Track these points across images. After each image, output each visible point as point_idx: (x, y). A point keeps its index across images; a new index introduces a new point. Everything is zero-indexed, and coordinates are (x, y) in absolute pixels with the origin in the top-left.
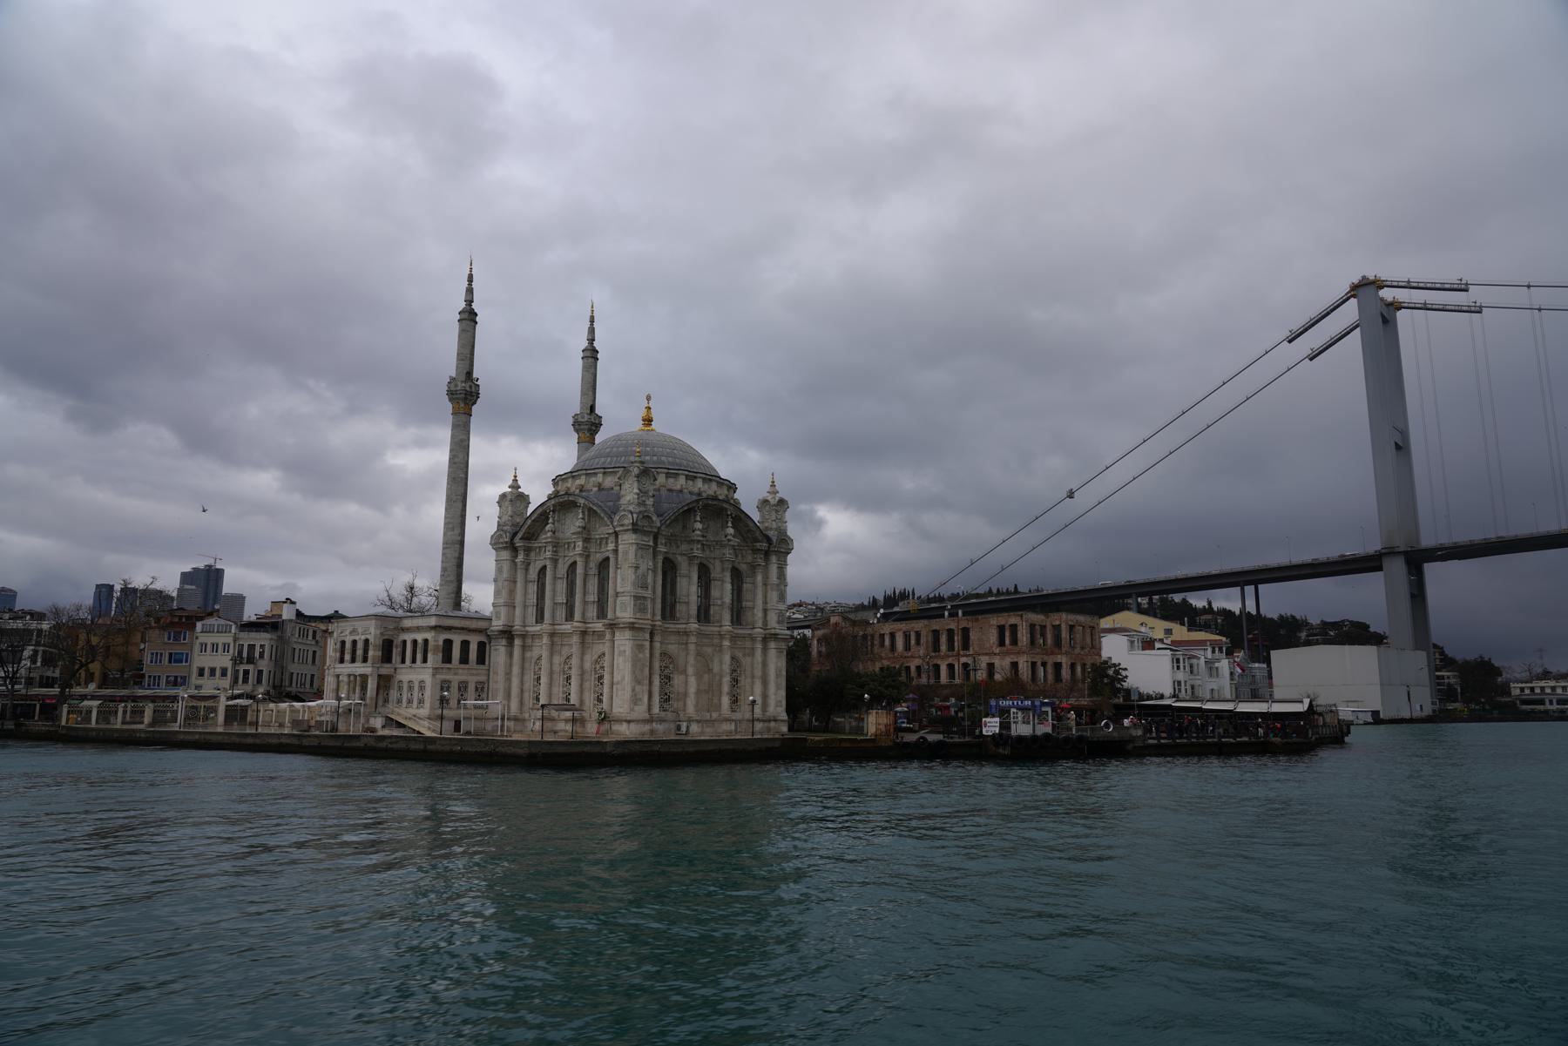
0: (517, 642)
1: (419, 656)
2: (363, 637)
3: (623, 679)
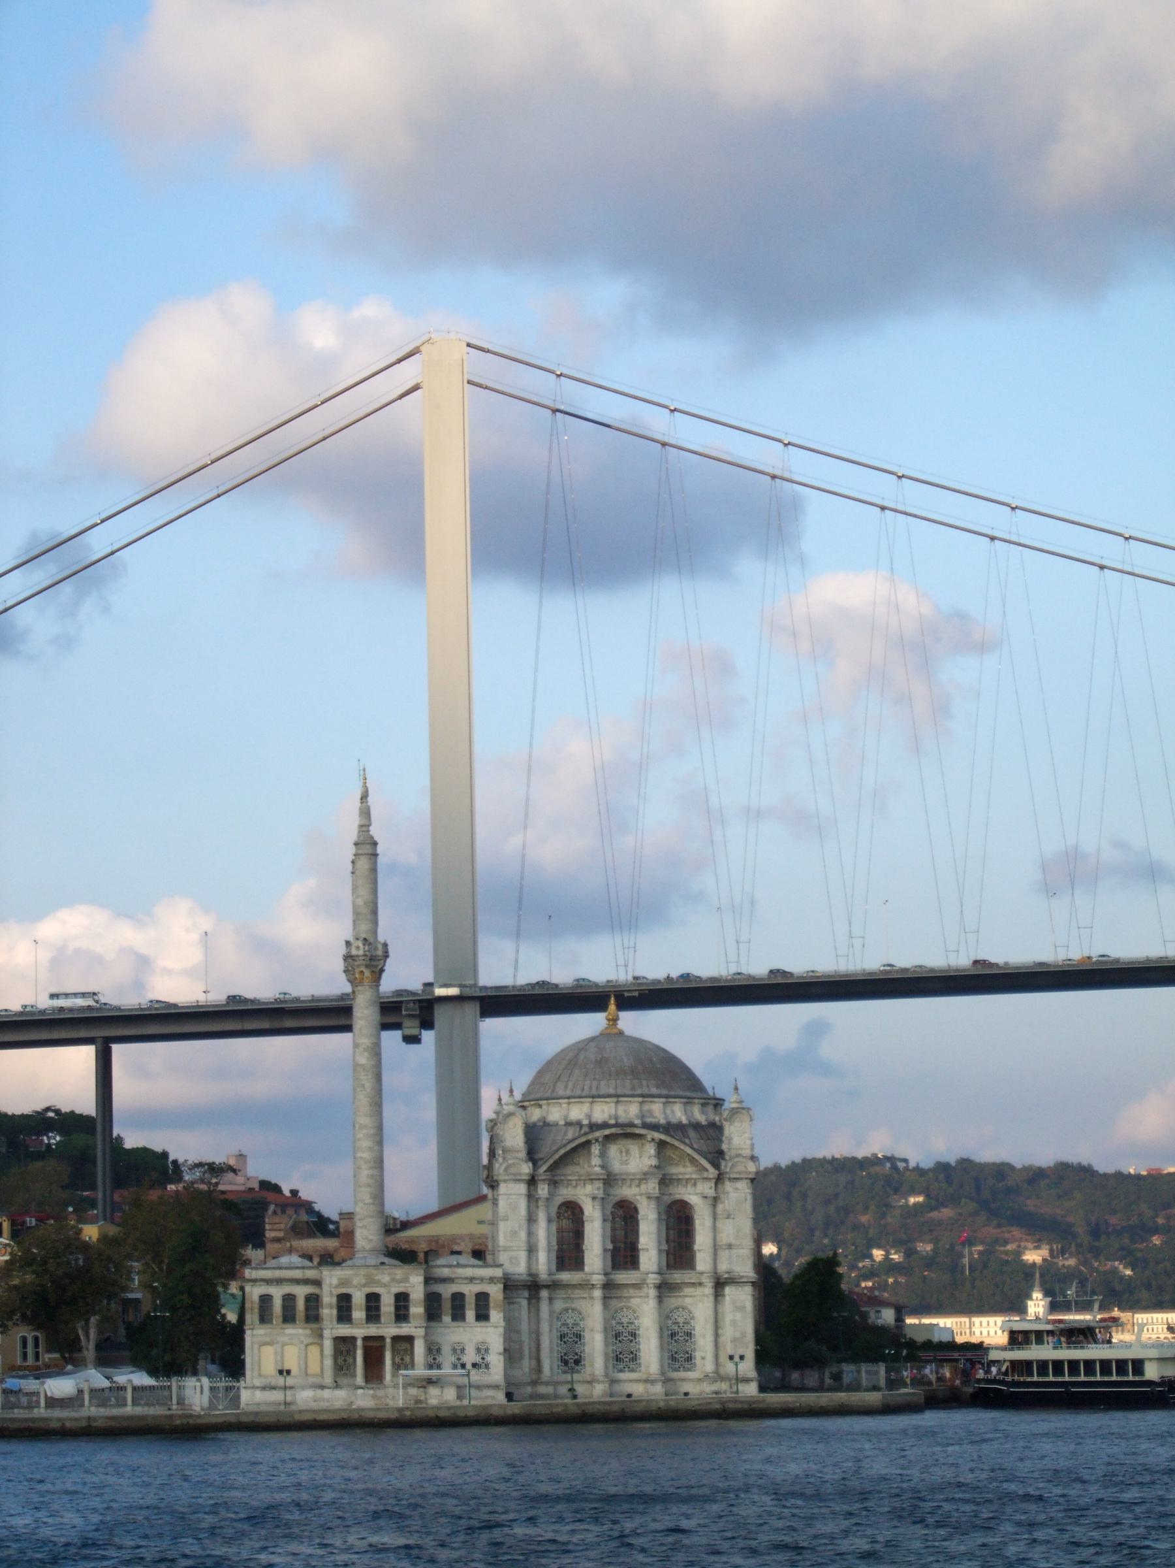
0: (544, 1294)
1: (470, 1314)
3: (744, 1335)
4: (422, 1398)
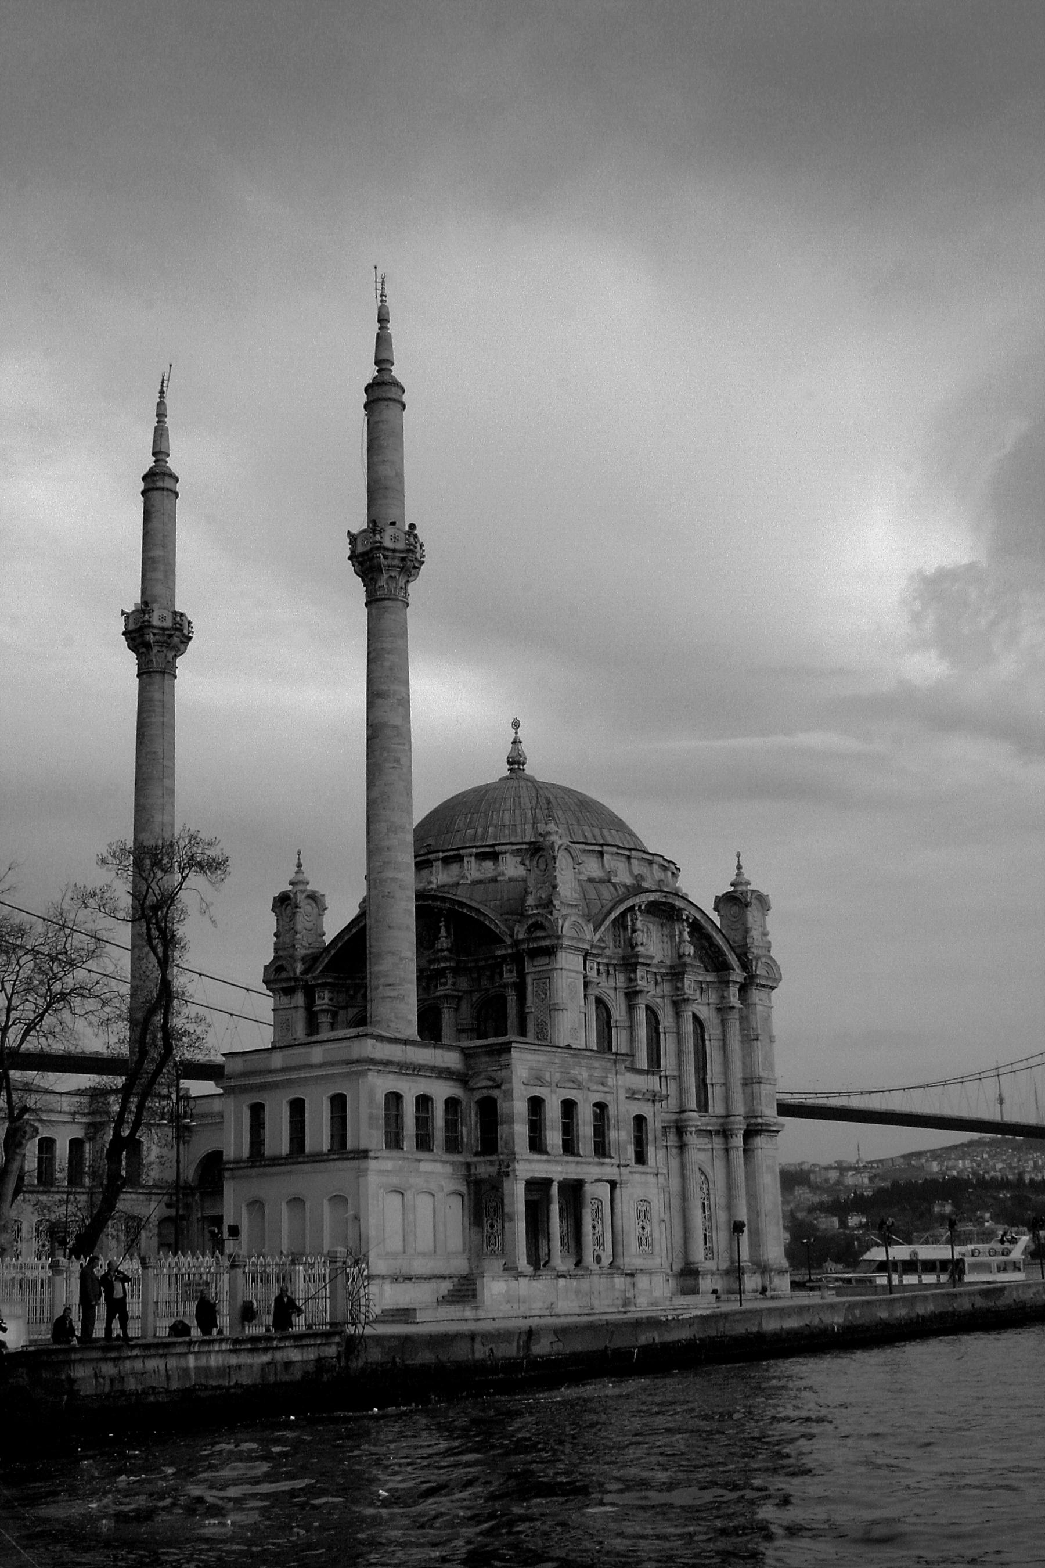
2: (597, 1098)
4: (630, 1295)
